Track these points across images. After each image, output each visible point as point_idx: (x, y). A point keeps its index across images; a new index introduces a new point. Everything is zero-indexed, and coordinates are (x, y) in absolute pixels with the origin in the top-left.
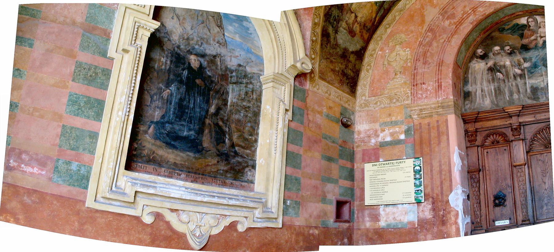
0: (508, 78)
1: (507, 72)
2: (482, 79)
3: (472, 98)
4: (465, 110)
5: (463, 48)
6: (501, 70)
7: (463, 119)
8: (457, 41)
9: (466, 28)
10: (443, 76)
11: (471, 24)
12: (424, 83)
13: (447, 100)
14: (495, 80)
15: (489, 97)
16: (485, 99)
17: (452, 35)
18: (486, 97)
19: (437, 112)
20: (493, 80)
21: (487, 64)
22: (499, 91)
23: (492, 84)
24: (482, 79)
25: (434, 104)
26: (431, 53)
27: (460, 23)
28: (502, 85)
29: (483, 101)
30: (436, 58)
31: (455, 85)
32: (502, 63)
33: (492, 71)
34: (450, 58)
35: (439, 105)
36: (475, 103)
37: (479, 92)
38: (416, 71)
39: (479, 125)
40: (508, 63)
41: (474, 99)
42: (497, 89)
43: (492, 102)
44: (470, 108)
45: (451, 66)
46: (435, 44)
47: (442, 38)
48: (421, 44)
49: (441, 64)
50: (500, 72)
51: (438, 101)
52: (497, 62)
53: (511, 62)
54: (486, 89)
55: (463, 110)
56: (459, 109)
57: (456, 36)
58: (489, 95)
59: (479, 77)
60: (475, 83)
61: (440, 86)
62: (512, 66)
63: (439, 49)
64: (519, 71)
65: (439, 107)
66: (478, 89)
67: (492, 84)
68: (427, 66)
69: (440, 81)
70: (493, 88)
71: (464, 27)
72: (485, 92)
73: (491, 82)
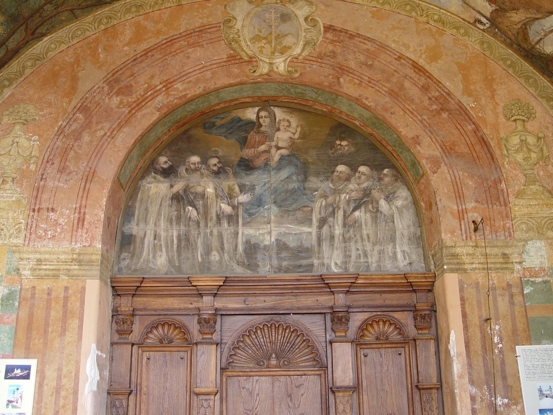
0: (206, 218)
1: (206, 206)
2: (159, 214)
3: (134, 249)
4: (120, 270)
5: (135, 153)
6: (196, 203)
7: (113, 287)
8: (126, 138)
9: (148, 116)
10: (89, 202)
11: (159, 110)
12: (53, 210)
13: (90, 250)
14: (183, 220)
15: (167, 252)
16: (159, 253)
17: (120, 127)
18: (161, 250)
19: (69, 270)
20: (179, 218)
21: (172, 186)
22: (185, 242)
23: (174, 227)
24: (159, 214)
25: (65, 253)
26: (76, 152)
27: (139, 105)
28: (193, 231)
29: (154, 256)
30: (83, 165)
31: (108, 221)
32: (199, 189)
33: (178, 201)
34: (108, 169)
35: (75, 256)
36: (139, 258)
37: (149, 238)
38: (42, 183)
39: (140, 301)
40: (210, 190)
41: (138, 251)
42: (183, 237)
43: (170, 261)
44: (128, 267)
45: (109, 185)
46: (86, 138)
47: (102, 129)
48: (61, 131)
49: (90, 178)
50: (194, 206)
51: (73, 250)
52: (191, 185)
53: (216, 189)
54: (163, 234)
55: (116, 269)
56: (110, 267)
57: (126, 129)
58: (167, 247)
59: (153, 209)
60: (146, 221)
61: (81, 221)
62: (217, 197)
63: (93, 148)
64: (227, 209)
65: (73, 260)
66: (149, 232)
67: (174, 227)
68: (64, 177)
69: (82, 211)
70: (175, 234)
71: (144, 116)
72: (160, 241)
73: (174, 223)
